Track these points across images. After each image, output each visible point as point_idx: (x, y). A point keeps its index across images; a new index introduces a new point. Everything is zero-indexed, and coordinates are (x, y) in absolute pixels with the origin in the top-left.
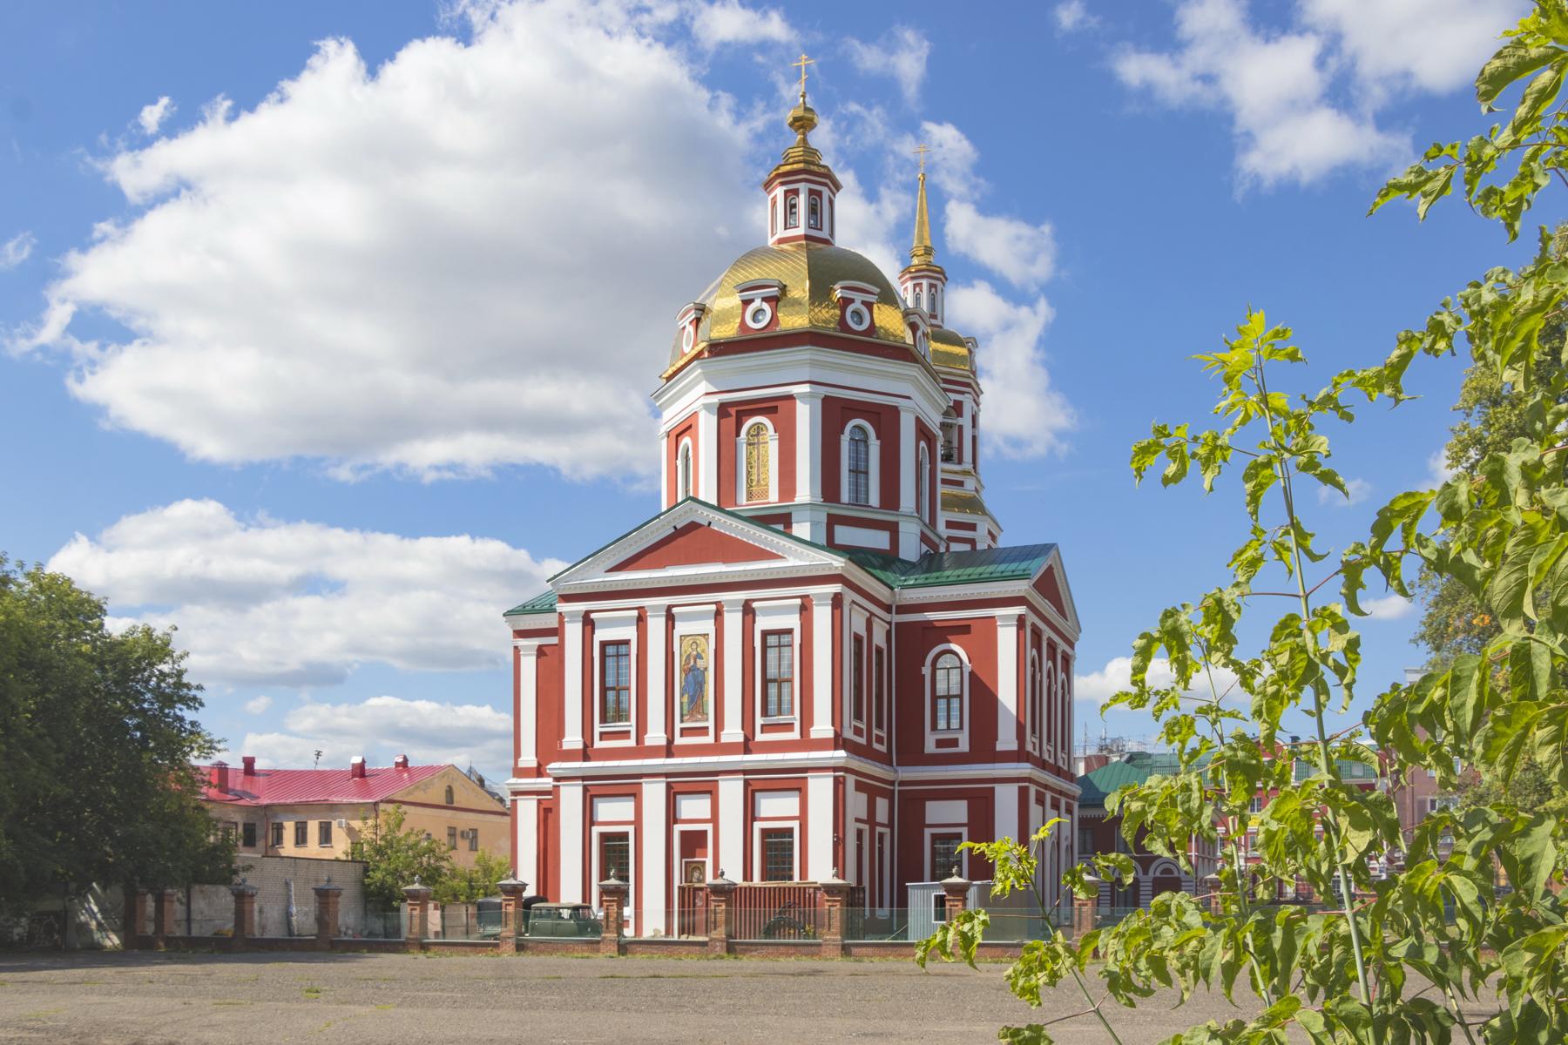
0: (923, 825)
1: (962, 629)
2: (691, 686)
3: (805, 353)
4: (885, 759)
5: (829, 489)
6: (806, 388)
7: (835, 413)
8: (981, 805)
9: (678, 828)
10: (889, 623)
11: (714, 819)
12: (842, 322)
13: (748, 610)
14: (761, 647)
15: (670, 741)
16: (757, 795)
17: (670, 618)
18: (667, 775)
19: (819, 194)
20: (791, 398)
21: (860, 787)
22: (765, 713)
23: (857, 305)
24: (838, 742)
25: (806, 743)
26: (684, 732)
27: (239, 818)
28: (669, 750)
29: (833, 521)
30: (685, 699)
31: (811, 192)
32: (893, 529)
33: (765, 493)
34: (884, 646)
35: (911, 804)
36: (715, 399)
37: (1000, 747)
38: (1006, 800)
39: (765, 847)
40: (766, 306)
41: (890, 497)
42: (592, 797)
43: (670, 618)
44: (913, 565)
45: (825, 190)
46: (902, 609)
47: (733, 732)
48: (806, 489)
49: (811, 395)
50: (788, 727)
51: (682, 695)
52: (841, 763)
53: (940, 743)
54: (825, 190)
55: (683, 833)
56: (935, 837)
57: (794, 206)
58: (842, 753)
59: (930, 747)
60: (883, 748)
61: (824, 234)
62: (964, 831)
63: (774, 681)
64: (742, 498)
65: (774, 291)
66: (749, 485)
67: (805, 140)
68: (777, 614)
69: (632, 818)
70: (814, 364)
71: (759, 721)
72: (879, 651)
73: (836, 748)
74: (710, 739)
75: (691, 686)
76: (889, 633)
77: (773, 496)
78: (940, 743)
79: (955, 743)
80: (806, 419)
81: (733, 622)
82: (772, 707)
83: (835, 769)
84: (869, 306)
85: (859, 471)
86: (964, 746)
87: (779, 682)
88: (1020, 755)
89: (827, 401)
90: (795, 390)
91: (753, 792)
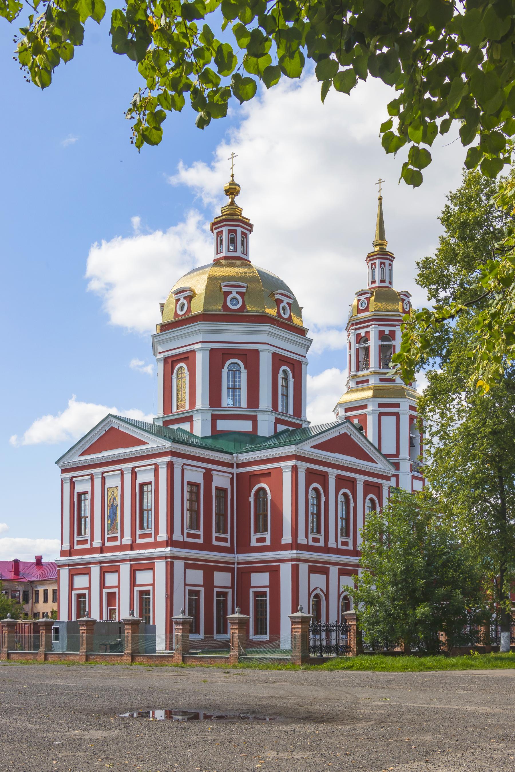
0: (249, 586)
1: (267, 474)
2: (111, 513)
3: (198, 326)
4: (230, 550)
5: (215, 399)
6: (199, 346)
7: (218, 357)
8: (274, 573)
9: (105, 591)
10: (233, 474)
11: (118, 587)
12: (225, 306)
13: (134, 474)
14: (140, 490)
15: (103, 544)
16: (106, 574)
17: (103, 479)
18: (100, 563)
19: (235, 231)
20: (193, 351)
21: (187, 566)
23: (234, 294)
24: (171, 543)
25: (156, 544)
26: (110, 539)
27: (21, 588)
28: (102, 550)
29: (215, 418)
30: (109, 522)
31: (230, 231)
32: (254, 419)
33: (184, 406)
34: (228, 486)
35: (242, 575)
36: (161, 356)
37: (283, 542)
38: (286, 570)
39: (141, 600)
40: (185, 302)
41: (253, 400)
42: (104, 573)
43: (103, 479)
44: (266, 439)
45: (239, 230)
46: (239, 466)
48: (202, 400)
49: (202, 349)
50: (149, 535)
51: (108, 520)
52: (168, 554)
53: (258, 540)
54: (239, 230)
55: (109, 594)
56: (256, 594)
57: (221, 241)
58: (168, 549)
59: (253, 543)
60: (228, 544)
61: (238, 254)
62: (267, 590)
63: (145, 510)
64: (174, 410)
65: (187, 294)
66: (177, 402)
67: (233, 203)
69: (88, 586)
70: (204, 331)
71: (138, 532)
72: (221, 491)
73: (167, 546)
74: (118, 543)
75: (111, 513)
76: (232, 479)
77: (187, 408)
78: (258, 540)
79: (263, 540)
80: (202, 361)
81: (128, 477)
82: (145, 525)
83: (166, 558)
84: (241, 294)
85: (234, 389)
86: (268, 542)
87: (148, 510)
88: (295, 545)
89: (212, 350)
90: (196, 347)
91: (134, 571)
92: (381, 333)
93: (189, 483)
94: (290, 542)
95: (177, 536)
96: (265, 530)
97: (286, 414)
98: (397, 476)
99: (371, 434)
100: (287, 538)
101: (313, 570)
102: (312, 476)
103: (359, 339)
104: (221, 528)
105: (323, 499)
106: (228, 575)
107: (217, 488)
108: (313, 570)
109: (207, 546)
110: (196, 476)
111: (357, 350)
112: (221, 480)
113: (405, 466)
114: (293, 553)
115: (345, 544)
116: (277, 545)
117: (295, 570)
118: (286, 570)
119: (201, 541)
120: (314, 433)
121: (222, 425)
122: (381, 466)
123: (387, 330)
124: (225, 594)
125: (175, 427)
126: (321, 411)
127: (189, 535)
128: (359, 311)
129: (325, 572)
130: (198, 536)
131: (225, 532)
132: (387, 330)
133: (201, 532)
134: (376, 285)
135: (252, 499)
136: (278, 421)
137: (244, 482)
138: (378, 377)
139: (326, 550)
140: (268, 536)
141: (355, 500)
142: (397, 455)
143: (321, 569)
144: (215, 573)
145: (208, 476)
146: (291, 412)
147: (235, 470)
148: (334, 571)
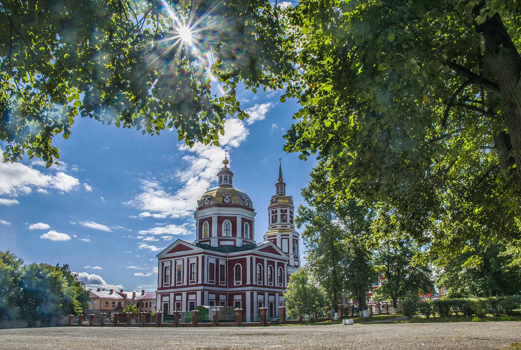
4: (226, 287)
5: (219, 234)
8: (243, 294)
21: (209, 293)
22: (191, 279)
24: (203, 284)
25: (197, 285)
29: (219, 241)
32: (235, 241)
35: (231, 296)
38: (248, 294)
46: (229, 257)
47: (185, 284)
53: (237, 283)
59: (235, 284)
60: (225, 285)
64: (203, 237)
68: (193, 260)
76: (226, 262)
78: (237, 283)
79: (239, 283)
86: (241, 284)
87: (194, 273)
92: (282, 211)
93: (210, 263)
94: (250, 284)
95: (206, 282)
96: (240, 280)
97: (247, 239)
98: (289, 260)
99: (279, 244)
100: (248, 282)
101: (258, 294)
102: (258, 261)
103: (273, 212)
104: (222, 279)
105: (262, 269)
106: (225, 296)
107: (221, 265)
108: (258, 294)
109: (217, 285)
110: (213, 261)
111: (272, 216)
112: (222, 262)
113: (292, 256)
114: (251, 288)
115: (271, 284)
116: (244, 285)
117: (252, 294)
118: (248, 294)
119: (215, 284)
120: (258, 246)
121: (222, 243)
122: (284, 257)
123: (284, 209)
124: (224, 303)
125: (203, 243)
126: (260, 238)
127: (210, 282)
128: (273, 203)
129: (263, 294)
130: (213, 282)
131: (224, 281)
132: (284, 209)
133: (215, 281)
134: (280, 193)
135: (234, 269)
136: (244, 241)
137: (231, 263)
138: (280, 225)
139: (264, 286)
140: (241, 282)
141: (274, 269)
142: (288, 253)
143: (261, 293)
144: (220, 296)
145: (217, 261)
146: (249, 238)
147: (228, 259)
148: (266, 294)
